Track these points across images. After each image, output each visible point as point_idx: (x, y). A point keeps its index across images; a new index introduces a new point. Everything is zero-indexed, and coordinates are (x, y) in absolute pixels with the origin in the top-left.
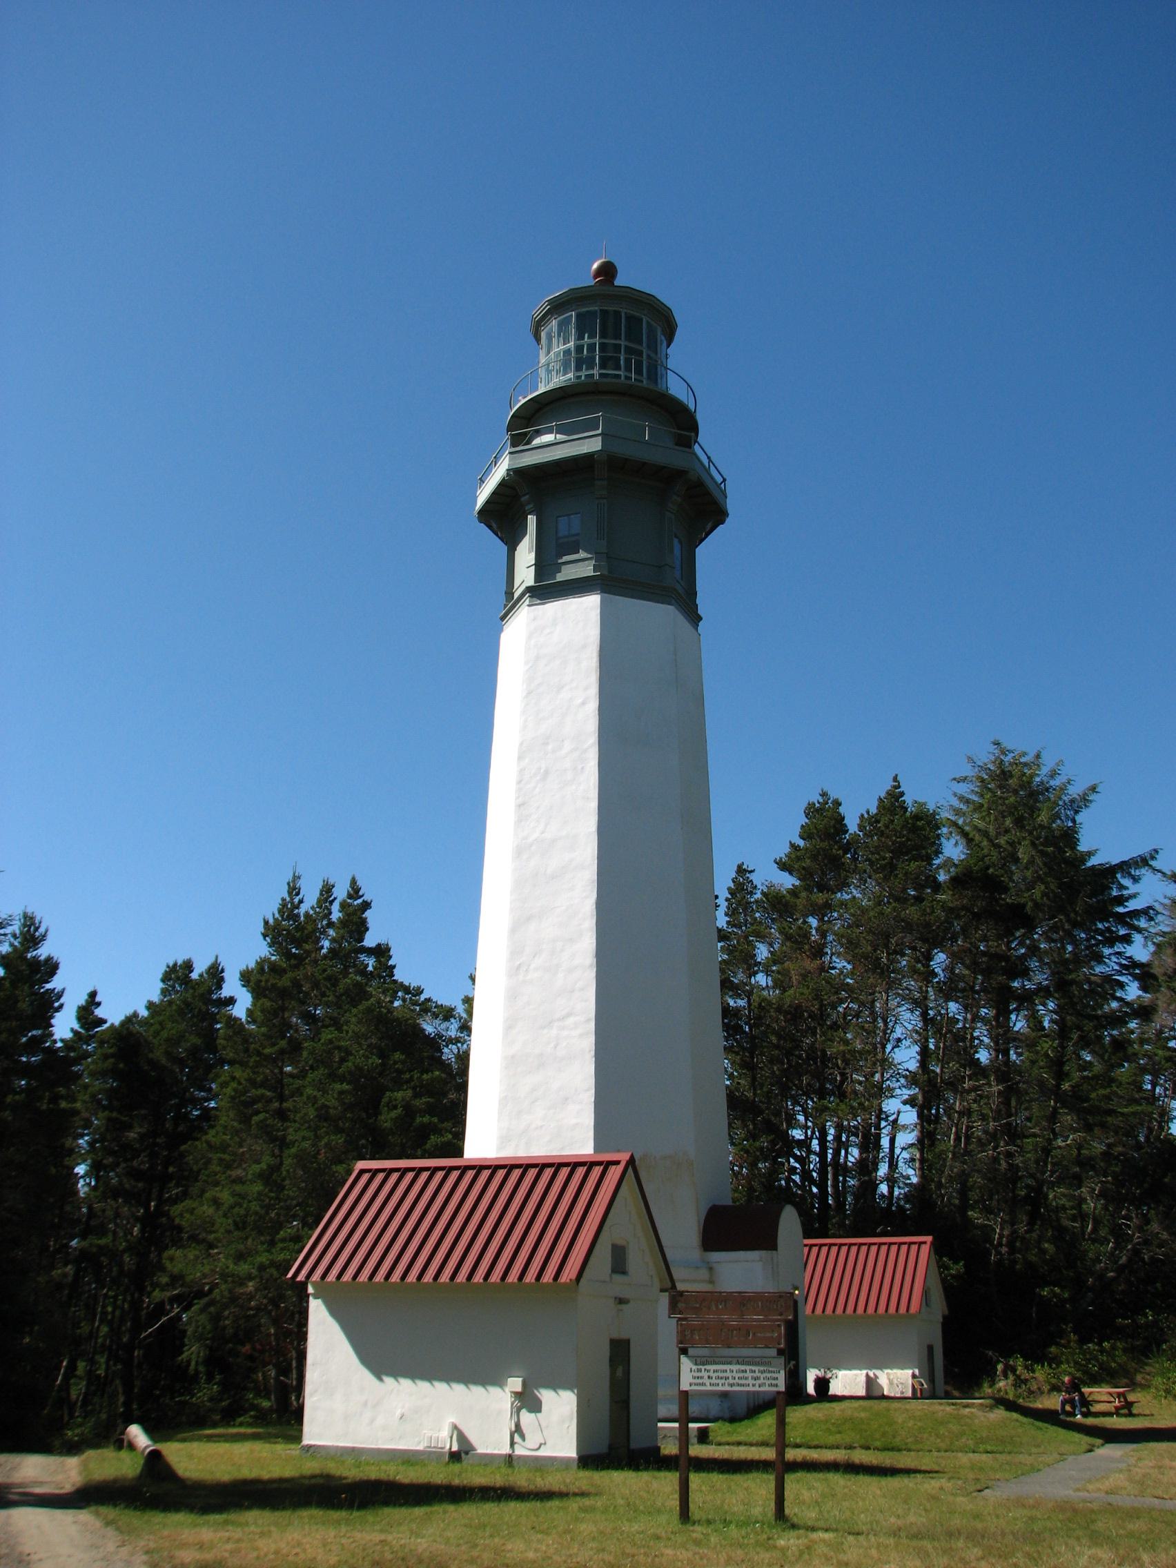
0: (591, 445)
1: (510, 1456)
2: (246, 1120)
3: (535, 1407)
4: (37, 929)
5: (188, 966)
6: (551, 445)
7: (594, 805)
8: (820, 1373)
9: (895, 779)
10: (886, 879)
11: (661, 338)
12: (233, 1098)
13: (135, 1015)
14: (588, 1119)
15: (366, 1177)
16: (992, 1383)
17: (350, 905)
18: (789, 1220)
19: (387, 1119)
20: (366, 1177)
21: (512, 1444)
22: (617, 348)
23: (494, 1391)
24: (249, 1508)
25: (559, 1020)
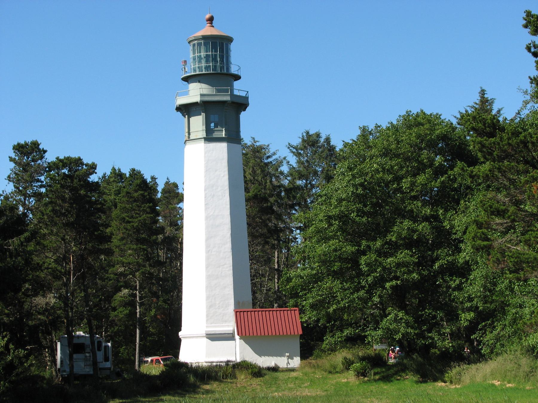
3: (292, 359)
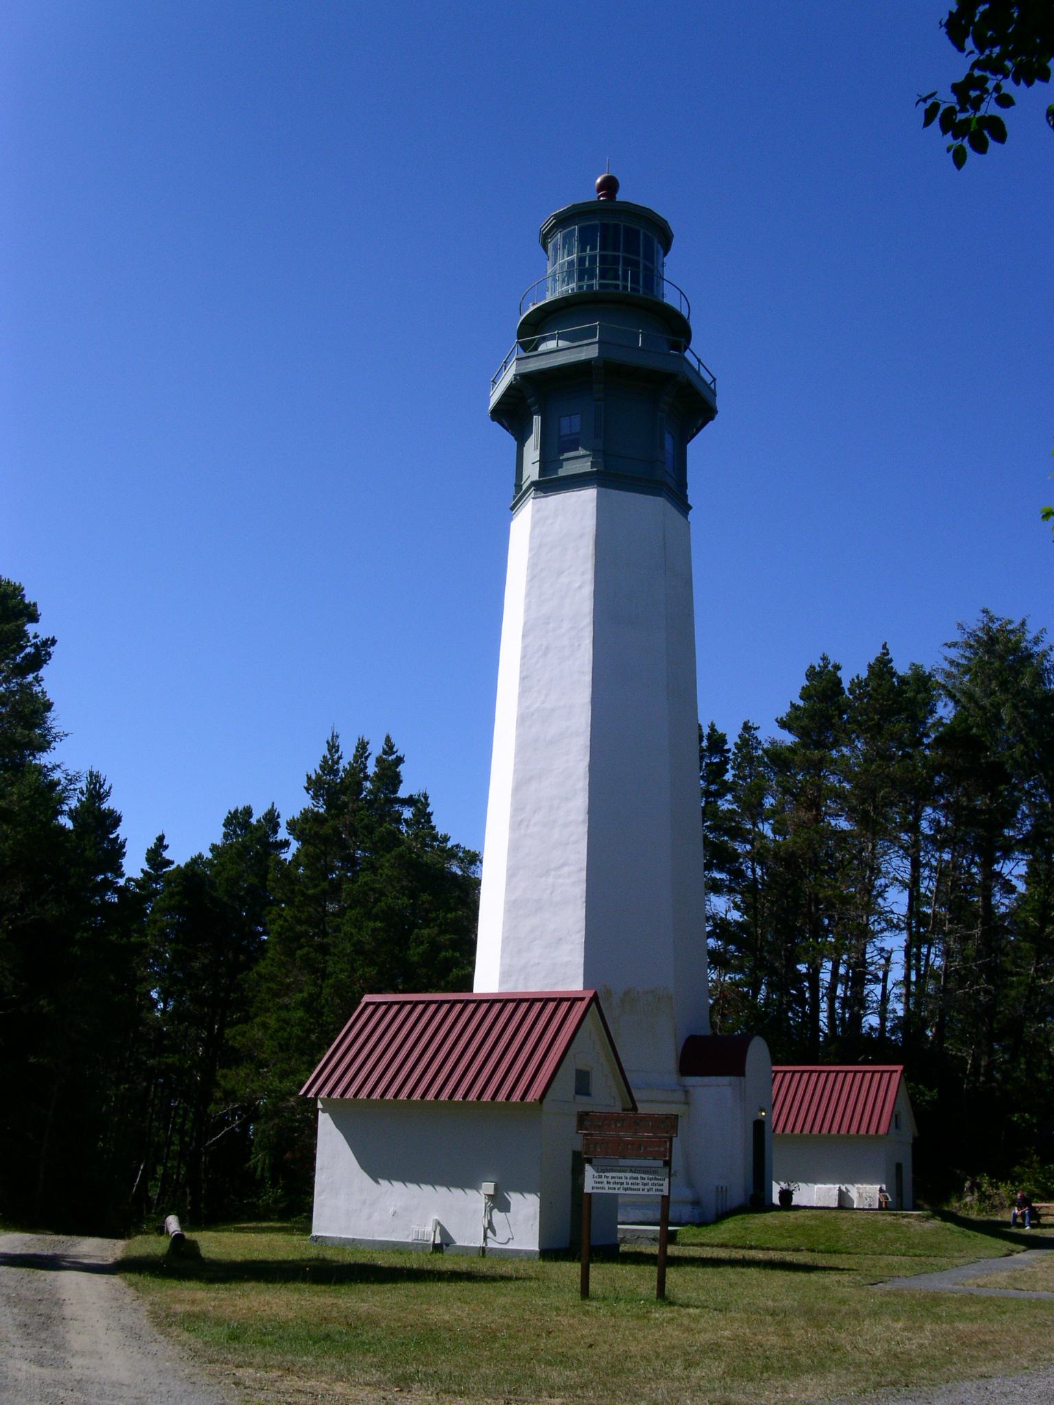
0: (589, 352)
1: (483, 1248)
2: (291, 954)
3: (505, 1207)
4: (101, 786)
5: (248, 812)
6: (555, 351)
7: (588, 678)
8: (784, 1185)
9: (884, 647)
10: (873, 738)
11: (658, 247)
12: (279, 934)
13: (200, 856)
14: (578, 958)
15: (371, 1008)
16: (960, 1199)
17: (384, 760)
18: (758, 1050)
19: (415, 953)
20: (371, 1008)
21: (485, 1238)
22: (616, 259)
23: (471, 1193)
24: (248, 1280)
25: (555, 869)
